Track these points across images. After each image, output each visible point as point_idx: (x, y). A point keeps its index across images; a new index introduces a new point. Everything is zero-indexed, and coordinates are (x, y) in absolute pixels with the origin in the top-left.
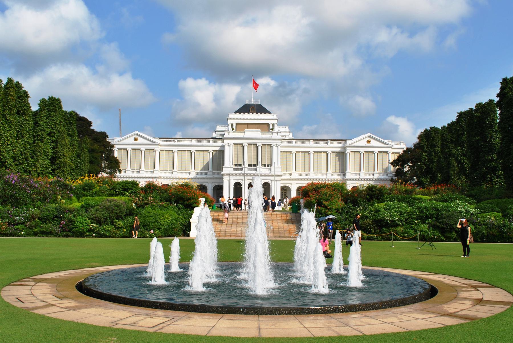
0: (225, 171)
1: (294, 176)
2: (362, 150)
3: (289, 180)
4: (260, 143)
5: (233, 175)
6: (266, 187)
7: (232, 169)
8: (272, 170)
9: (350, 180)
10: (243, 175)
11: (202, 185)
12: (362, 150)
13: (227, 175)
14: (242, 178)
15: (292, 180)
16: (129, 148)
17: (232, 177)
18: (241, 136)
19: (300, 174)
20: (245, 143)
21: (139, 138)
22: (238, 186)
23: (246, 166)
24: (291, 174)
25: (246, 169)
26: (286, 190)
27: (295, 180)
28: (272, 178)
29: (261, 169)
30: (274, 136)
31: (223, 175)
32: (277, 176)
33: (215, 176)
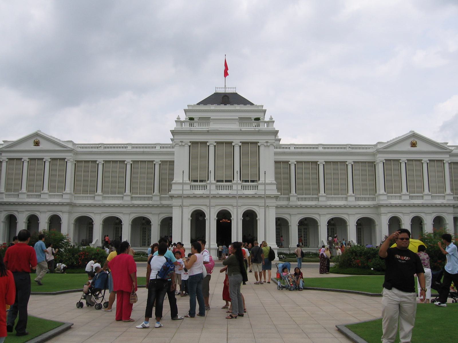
0: (176, 190)
1: (294, 201)
2: (403, 158)
3: (287, 207)
4: (237, 140)
5: (188, 197)
6: (250, 219)
7: (187, 187)
8: (261, 187)
9: (387, 206)
10: (208, 197)
11: (144, 218)
12: (403, 158)
13: (179, 197)
14: (206, 201)
15: (291, 207)
16: (26, 157)
17: (187, 202)
18: (204, 128)
19: (305, 199)
20: (211, 140)
21: (41, 141)
22: (201, 218)
23: (213, 181)
24: (289, 199)
25: (213, 187)
26: (306, 225)
27: (296, 207)
28: (261, 202)
29: (239, 187)
30: (263, 127)
31: (172, 197)
32: (269, 197)
33: (165, 202)
